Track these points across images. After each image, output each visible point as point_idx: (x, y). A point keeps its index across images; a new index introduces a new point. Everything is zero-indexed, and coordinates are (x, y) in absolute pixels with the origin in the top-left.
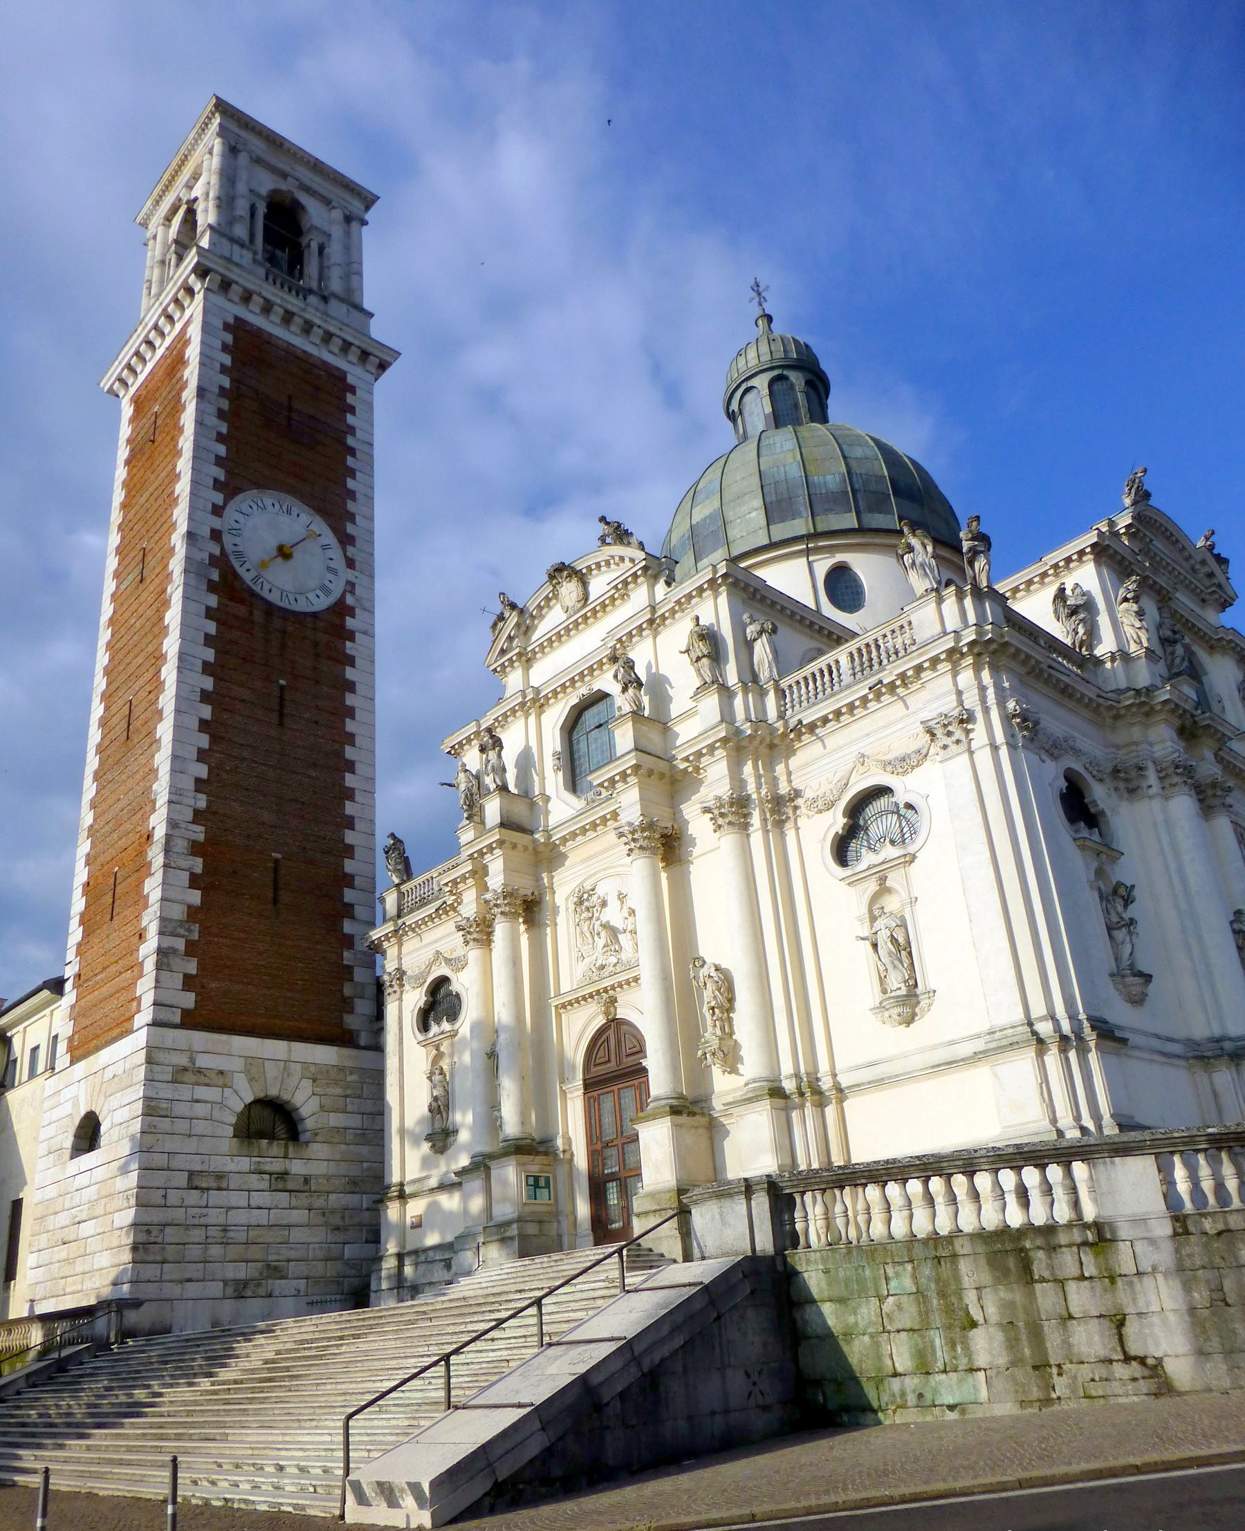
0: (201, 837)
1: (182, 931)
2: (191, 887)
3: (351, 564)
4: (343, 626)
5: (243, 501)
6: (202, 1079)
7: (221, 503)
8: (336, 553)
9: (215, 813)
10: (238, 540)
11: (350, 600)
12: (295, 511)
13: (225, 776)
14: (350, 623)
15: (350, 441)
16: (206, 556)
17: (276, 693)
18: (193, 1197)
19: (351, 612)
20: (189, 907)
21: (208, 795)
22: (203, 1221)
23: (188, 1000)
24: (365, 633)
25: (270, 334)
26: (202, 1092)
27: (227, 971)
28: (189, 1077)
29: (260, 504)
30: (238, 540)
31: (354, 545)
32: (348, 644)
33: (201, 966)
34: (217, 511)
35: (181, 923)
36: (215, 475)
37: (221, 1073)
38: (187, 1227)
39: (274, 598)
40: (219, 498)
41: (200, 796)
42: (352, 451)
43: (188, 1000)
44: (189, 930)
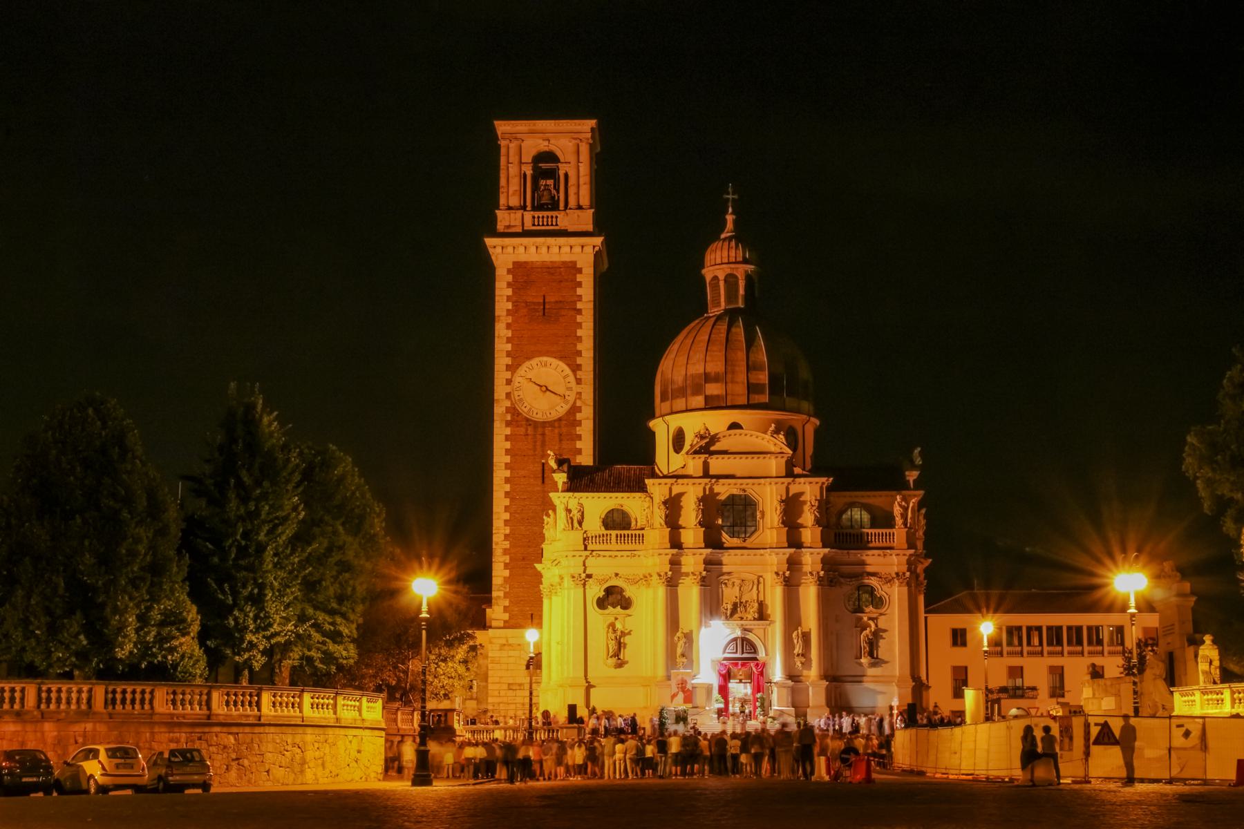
0: (508, 546)
1: (501, 588)
2: (505, 569)
3: (579, 381)
4: (575, 420)
5: (522, 371)
6: (511, 647)
7: (510, 377)
8: (572, 378)
9: (514, 534)
10: (520, 393)
11: (579, 403)
12: (548, 365)
13: (517, 516)
14: (579, 416)
15: (579, 305)
16: (504, 408)
17: (541, 466)
18: (510, 693)
19: (579, 410)
20: (505, 578)
21: (510, 526)
22: (515, 702)
23: (506, 616)
24: (587, 419)
25: (532, 262)
26: (512, 653)
27: (522, 603)
28: (506, 647)
29: (531, 367)
30: (520, 393)
31: (581, 370)
32: (578, 428)
33: (510, 601)
34: (509, 382)
35: (501, 585)
36: (505, 363)
37: (519, 645)
38: (508, 704)
39: (539, 417)
40: (508, 375)
41: (506, 527)
42: (579, 312)
43: (506, 616)
44: (505, 588)
